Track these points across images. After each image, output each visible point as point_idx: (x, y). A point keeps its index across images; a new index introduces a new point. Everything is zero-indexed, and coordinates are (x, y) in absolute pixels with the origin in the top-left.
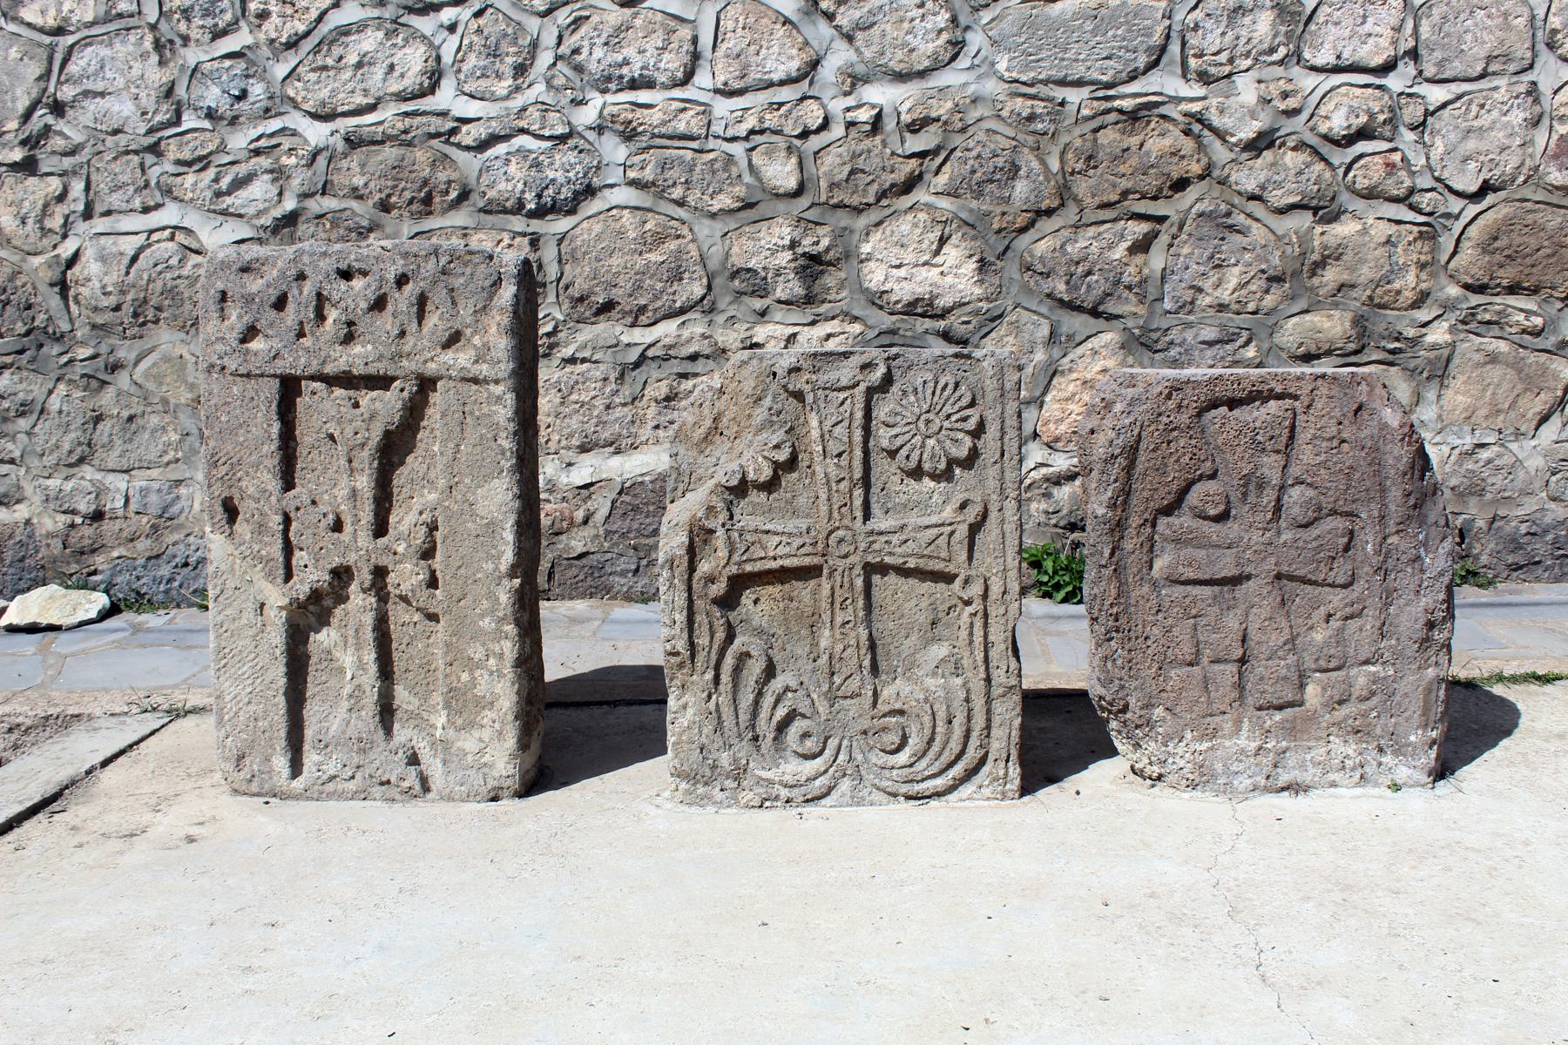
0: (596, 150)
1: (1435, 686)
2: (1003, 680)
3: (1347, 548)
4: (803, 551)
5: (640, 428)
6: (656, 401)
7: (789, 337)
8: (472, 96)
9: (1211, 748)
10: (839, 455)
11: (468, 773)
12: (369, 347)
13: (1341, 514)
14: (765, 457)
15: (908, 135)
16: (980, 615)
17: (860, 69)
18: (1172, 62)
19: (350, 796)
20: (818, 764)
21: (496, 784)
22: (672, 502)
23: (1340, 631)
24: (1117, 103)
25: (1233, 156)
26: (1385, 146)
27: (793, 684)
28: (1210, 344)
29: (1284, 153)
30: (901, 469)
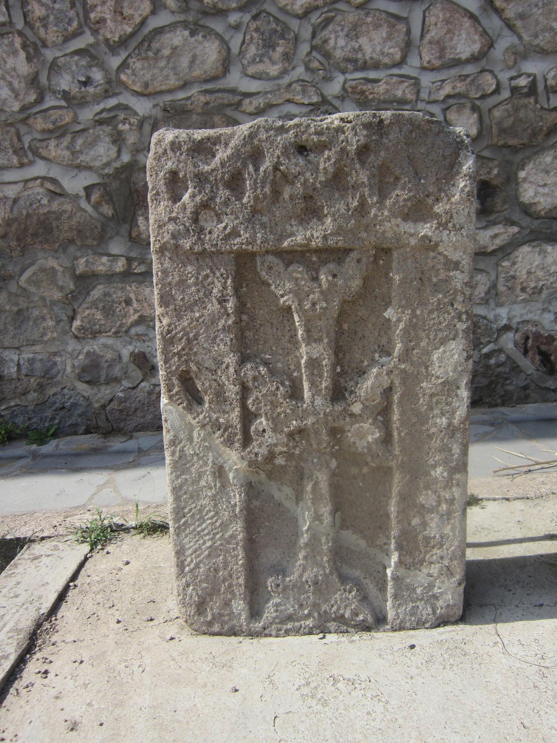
8: (253, 77)
11: (418, 603)
15: (551, 95)
17: (521, 48)
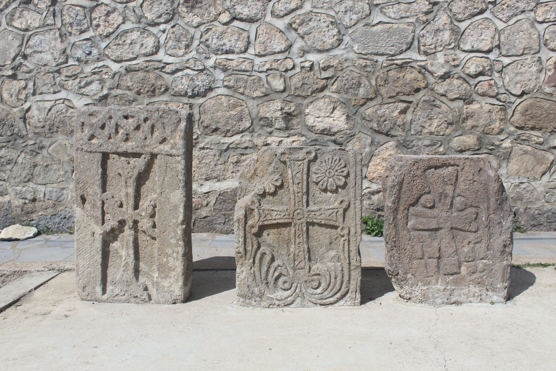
0: (213, 75)
1: (506, 267)
2: (355, 263)
3: (476, 219)
4: (285, 217)
5: (227, 172)
6: (232, 163)
7: (280, 141)
8: (170, 55)
9: (428, 289)
10: (298, 184)
11: (165, 294)
12: (134, 143)
13: (474, 207)
14: (272, 184)
15: (322, 72)
16: (347, 241)
17: (306, 48)
18: (415, 48)
19: (123, 301)
20: (289, 292)
21: (175, 298)
22: (239, 199)
23: (473, 248)
24: (395, 62)
25: (436, 81)
26: (488, 78)
27: (281, 264)
28: (427, 146)
29: (454, 80)
30: (320, 189)
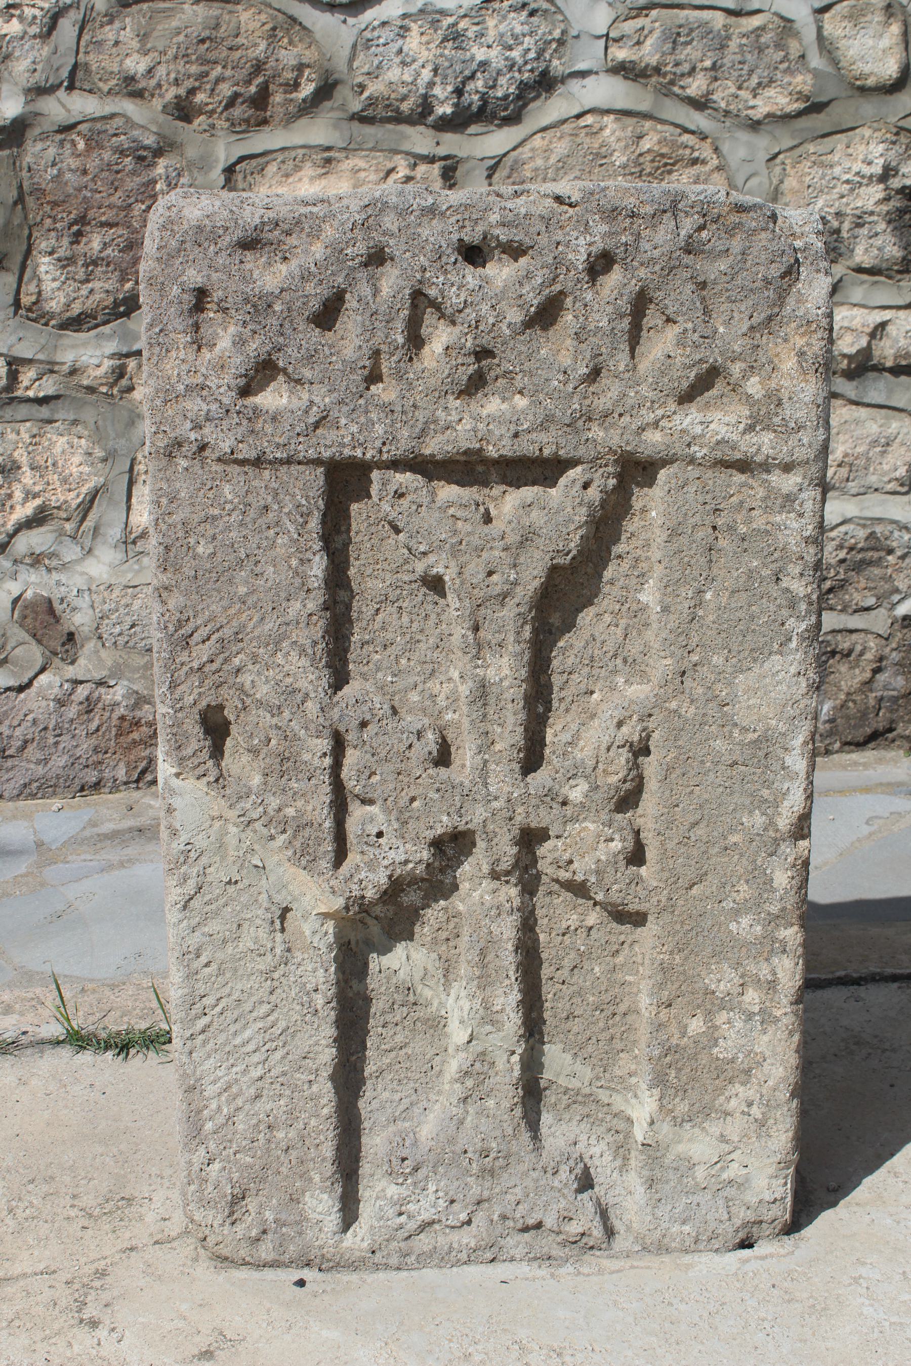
0: (559, 11)
7: (876, 328)
11: (695, 1199)
12: (521, 402)
19: (464, 1256)
21: (751, 1216)
